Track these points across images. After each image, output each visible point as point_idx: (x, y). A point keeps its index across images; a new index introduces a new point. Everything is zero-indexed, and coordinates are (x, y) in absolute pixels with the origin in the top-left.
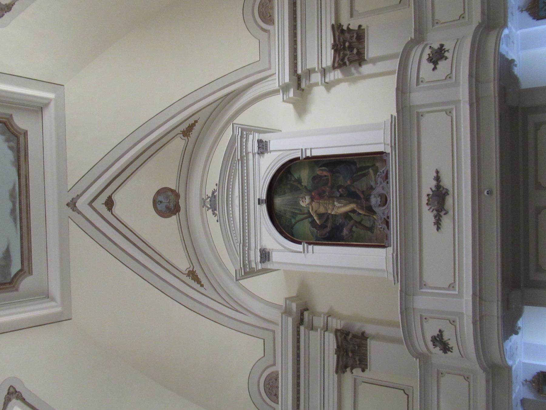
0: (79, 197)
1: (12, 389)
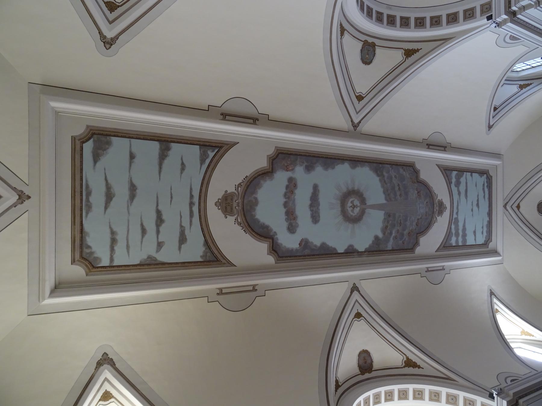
0: (15, 205)
1: (108, 46)
